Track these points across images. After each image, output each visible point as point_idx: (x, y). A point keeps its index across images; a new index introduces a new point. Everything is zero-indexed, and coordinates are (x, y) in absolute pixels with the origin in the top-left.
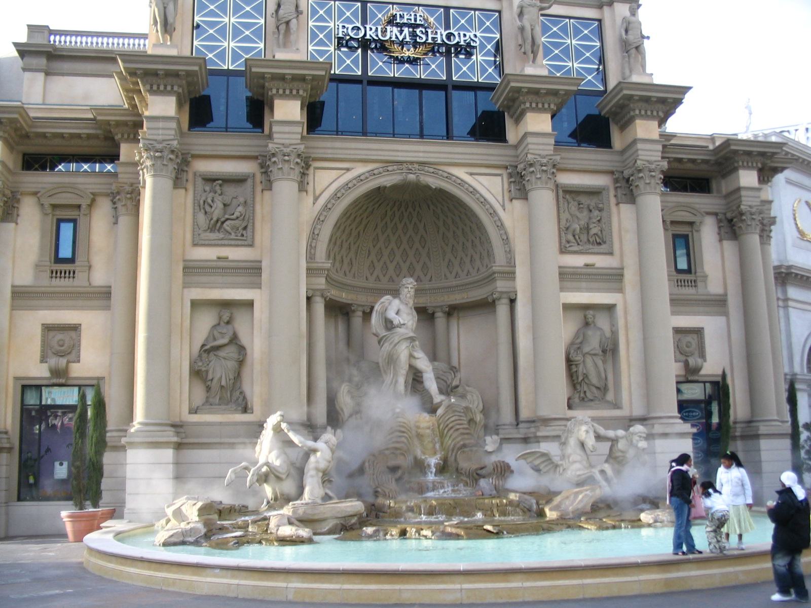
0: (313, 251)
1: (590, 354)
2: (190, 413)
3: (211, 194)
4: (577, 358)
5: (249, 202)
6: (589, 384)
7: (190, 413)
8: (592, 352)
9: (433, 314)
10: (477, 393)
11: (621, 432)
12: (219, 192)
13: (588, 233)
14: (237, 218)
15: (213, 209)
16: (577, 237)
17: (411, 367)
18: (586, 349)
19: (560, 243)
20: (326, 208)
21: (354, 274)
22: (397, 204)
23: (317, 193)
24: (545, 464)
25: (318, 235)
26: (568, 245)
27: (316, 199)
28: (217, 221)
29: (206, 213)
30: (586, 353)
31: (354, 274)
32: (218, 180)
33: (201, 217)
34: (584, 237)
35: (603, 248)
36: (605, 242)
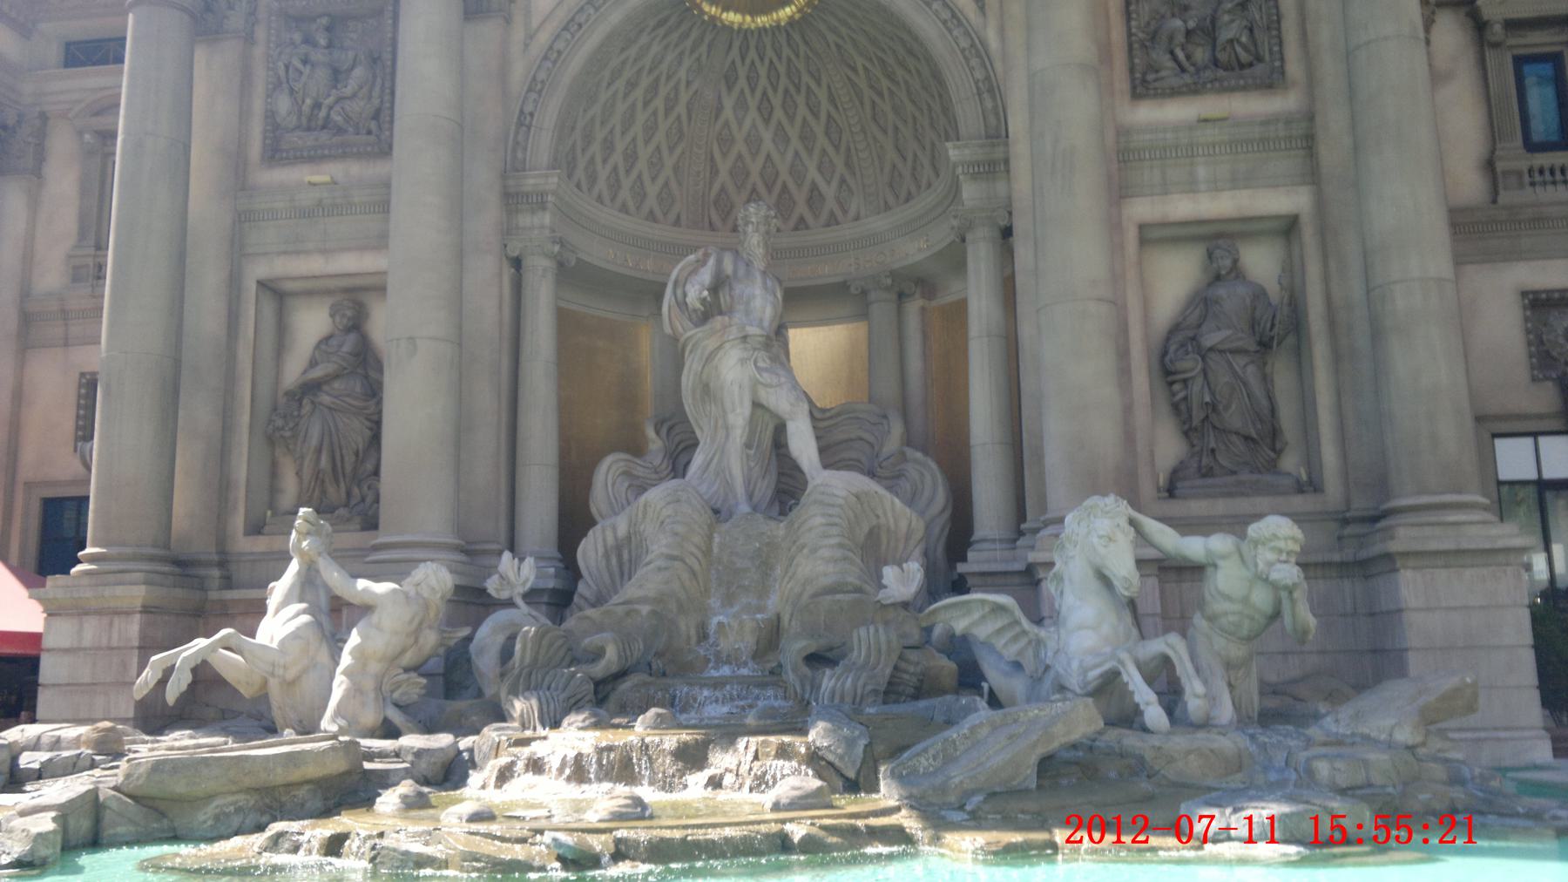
0: (520, 155)
1: (1222, 352)
2: (248, 533)
3: (304, 49)
4: (1187, 364)
5: (387, 56)
6: (1222, 431)
7: (248, 533)
8: (1221, 347)
9: (864, 293)
10: (933, 465)
11: (1219, 543)
12: (323, 42)
13: (1215, 40)
14: (354, 95)
15: (304, 79)
16: (1181, 55)
17: (757, 405)
18: (1211, 339)
19: (1132, 70)
20: (552, 56)
21: (678, 217)
22: (753, 43)
23: (535, 24)
24: (1009, 635)
25: (532, 115)
26: (1150, 77)
27: (530, 37)
28: (317, 106)
29: (292, 91)
30: (1211, 349)
31: (678, 217)
32: (320, 16)
33: (284, 104)
34: (1201, 54)
35: (1259, 69)
36: (1259, 59)
